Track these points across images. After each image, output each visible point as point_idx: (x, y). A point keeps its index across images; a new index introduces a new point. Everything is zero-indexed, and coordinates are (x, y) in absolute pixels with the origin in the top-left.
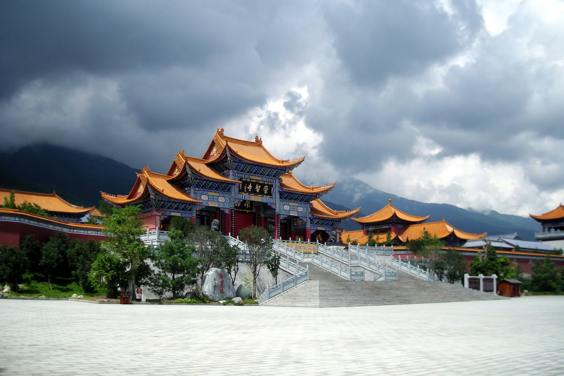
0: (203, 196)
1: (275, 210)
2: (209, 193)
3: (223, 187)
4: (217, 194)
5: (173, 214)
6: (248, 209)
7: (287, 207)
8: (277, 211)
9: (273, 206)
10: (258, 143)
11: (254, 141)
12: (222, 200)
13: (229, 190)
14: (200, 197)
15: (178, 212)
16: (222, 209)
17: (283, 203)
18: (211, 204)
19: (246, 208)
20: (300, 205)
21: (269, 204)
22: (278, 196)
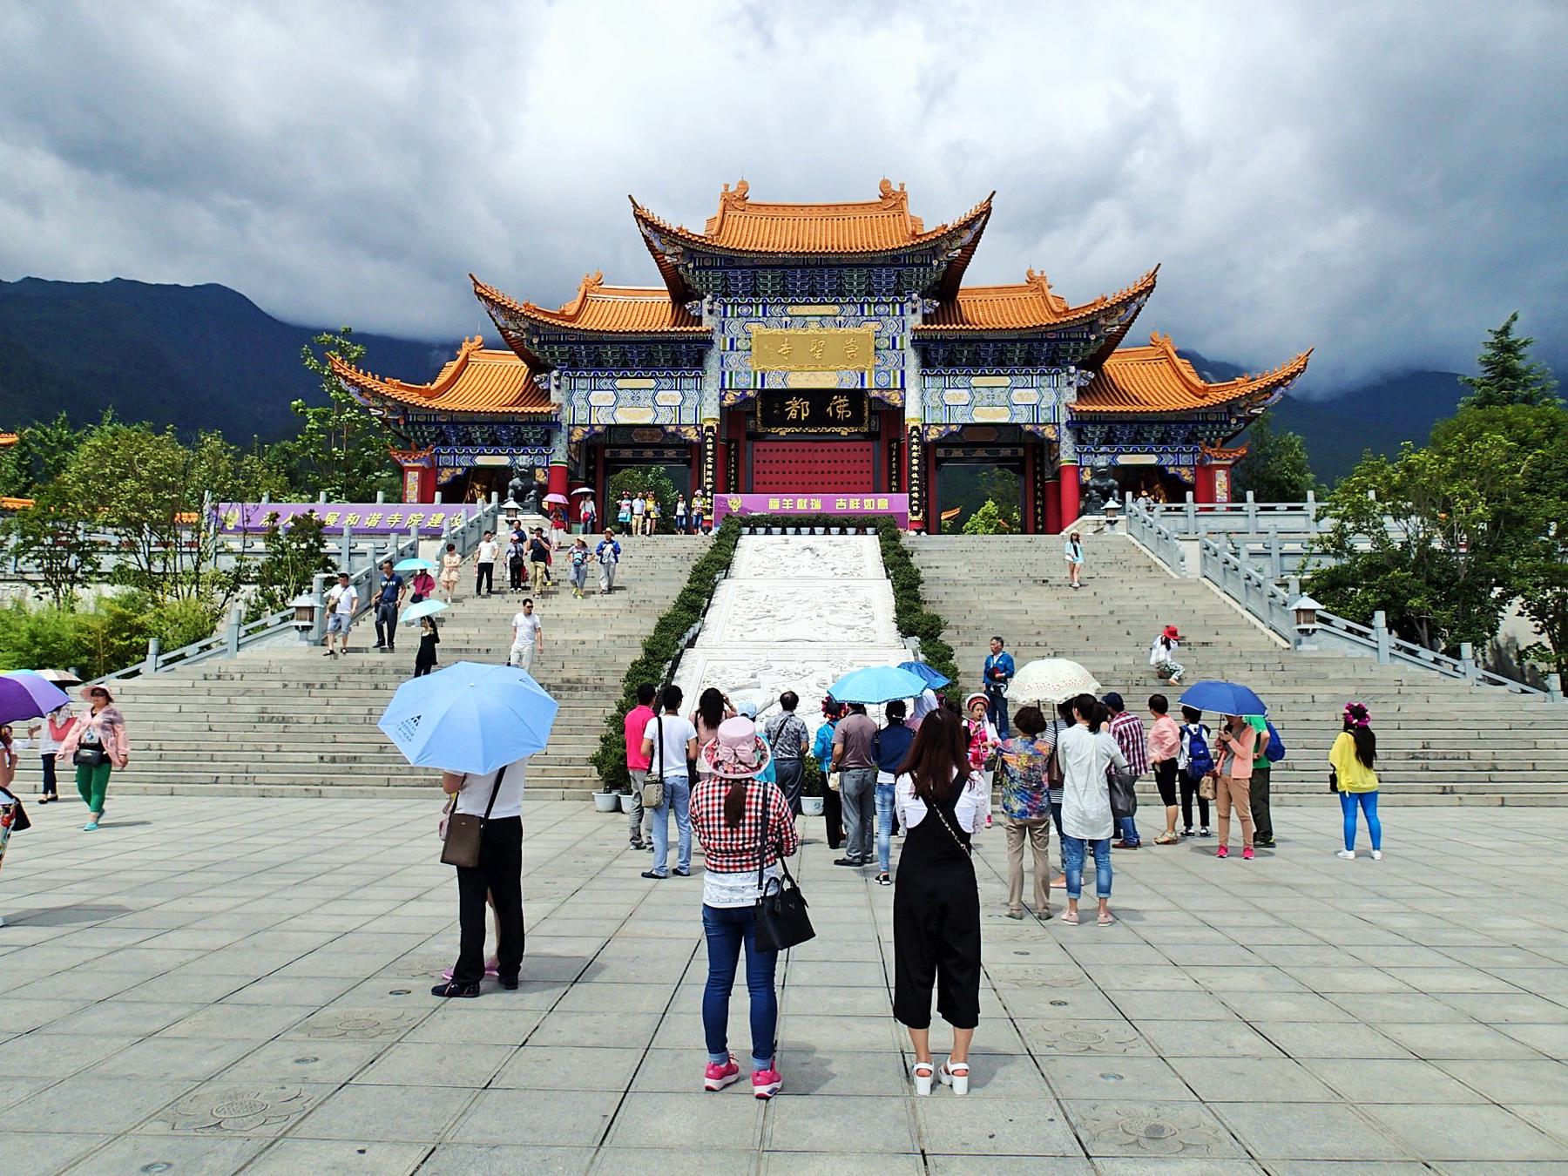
2: (619, 383)
3: (677, 355)
4: (652, 383)
5: (481, 461)
6: (847, 423)
8: (912, 415)
9: (895, 399)
10: (892, 199)
13: (699, 362)
14: (587, 400)
16: (671, 429)
17: (939, 381)
18: (627, 416)
19: (835, 422)
20: (1021, 381)
21: (875, 394)
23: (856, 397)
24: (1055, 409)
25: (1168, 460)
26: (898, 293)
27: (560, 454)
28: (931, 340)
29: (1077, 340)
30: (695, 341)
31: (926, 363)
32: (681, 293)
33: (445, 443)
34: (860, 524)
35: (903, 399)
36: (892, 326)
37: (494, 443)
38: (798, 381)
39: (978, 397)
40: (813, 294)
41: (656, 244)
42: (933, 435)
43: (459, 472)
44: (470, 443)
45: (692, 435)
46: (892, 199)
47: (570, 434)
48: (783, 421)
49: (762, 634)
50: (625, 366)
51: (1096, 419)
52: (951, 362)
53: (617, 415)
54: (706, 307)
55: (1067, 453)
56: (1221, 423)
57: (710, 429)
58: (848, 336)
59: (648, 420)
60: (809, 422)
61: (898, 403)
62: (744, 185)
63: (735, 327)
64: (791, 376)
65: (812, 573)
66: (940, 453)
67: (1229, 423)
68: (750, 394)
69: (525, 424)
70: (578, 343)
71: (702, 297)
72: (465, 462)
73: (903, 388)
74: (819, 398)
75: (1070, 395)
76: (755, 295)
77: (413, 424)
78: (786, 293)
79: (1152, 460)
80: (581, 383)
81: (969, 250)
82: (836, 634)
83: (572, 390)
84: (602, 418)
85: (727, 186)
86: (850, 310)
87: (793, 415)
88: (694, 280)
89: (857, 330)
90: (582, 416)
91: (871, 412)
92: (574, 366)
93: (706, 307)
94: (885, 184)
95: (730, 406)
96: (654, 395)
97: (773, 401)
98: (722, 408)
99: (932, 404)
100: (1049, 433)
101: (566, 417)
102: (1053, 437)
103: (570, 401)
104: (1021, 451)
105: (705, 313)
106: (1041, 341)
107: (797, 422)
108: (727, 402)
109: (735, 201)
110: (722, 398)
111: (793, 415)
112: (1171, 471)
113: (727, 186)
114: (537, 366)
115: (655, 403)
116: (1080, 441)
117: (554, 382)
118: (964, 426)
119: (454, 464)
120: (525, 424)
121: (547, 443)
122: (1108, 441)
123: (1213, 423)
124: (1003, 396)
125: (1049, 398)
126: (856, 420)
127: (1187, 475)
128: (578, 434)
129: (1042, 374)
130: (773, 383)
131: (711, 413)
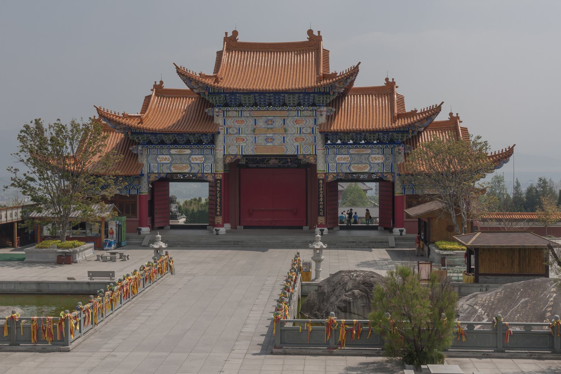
8: (321, 167)
10: (313, 43)
13: (213, 142)
16: (199, 175)
42: (330, 178)
46: (313, 43)
47: (149, 177)
53: (172, 169)
62: (235, 33)
85: (226, 33)
96: (190, 157)
98: (225, 165)
108: (227, 161)
109: (232, 43)
113: (226, 33)
115: (190, 161)
128: (153, 178)
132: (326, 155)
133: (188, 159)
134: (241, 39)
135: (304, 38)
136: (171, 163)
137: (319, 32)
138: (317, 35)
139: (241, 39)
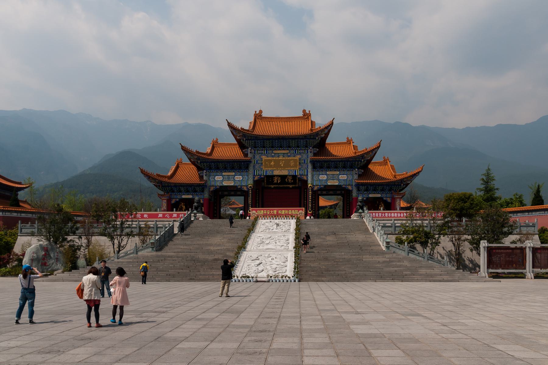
0: (216, 177)
1: (307, 181)
2: (223, 174)
4: (234, 174)
5: (184, 197)
6: (291, 184)
7: (323, 177)
8: (309, 181)
9: (305, 178)
11: (301, 114)
12: (239, 178)
14: (214, 178)
15: (188, 195)
16: (239, 187)
17: (318, 173)
18: (225, 184)
21: (299, 176)
22: (310, 167)
23: (294, 177)
24: (351, 181)
25: (384, 195)
26: (307, 147)
27: (206, 195)
28: (315, 161)
29: (358, 161)
30: (246, 161)
31: (314, 168)
32: (242, 146)
33: (173, 192)
34: (292, 216)
35: (307, 178)
36: (305, 156)
37: (187, 192)
38: (276, 173)
39: (329, 177)
40: (281, 147)
41: (234, 133)
42: (316, 188)
43: (177, 200)
44: (180, 191)
45: (245, 189)
48: (272, 183)
49: (261, 247)
50: (225, 169)
51: (363, 184)
52: (321, 167)
54: (249, 151)
55: (354, 194)
56: (399, 185)
57: (250, 187)
58: (291, 160)
59: (232, 184)
60: (280, 184)
61: (306, 179)
62: (261, 112)
63: (257, 157)
64: (275, 171)
65: (277, 231)
66: (319, 192)
67: (401, 185)
68: (262, 176)
69: (196, 186)
70: (212, 162)
71: (248, 148)
72: (179, 197)
73: (307, 175)
74: (283, 177)
75: (356, 177)
76: (264, 147)
77: (164, 186)
78: (273, 147)
79: (379, 196)
80: (212, 174)
81: (327, 135)
82: (278, 247)
83: (209, 176)
84: (219, 184)
85: (256, 112)
86: (292, 152)
87: (276, 181)
88: (246, 143)
89: (294, 158)
90: (213, 183)
91: (299, 181)
92: (210, 168)
93: (249, 151)
94: (304, 111)
95: (257, 180)
97: (270, 178)
98: (254, 181)
99: (317, 179)
100: (350, 188)
101: (209, 183)
102: (351, 189)
103: (209, 179)
104: (343, 192)
105: (249, 153)
106: (348, 161)
107: (277, 184)
108: (256, 179)
109: (258, 117)
110: (254, 178)
111: (276, 181)
112: (385, 199)
113: (256, 112)
114: (199, 169)
116: (359, 190)
117: (205, 174)
118: (325, 186)
119: (176, 197)
120: (196, 186)
121: (203, 191)
122: (367, 190)
123: (397, 185)
124: (337, 177)
125: (350, 177)
126: (294, 183)
127: (389, 200)
128: (212, 189)
129: (348, 170)
130: (269, 173)
131: (250, 183)
132: (313, 176)
133: (234, 178)
134: (264, 115)
135: (301, 114)
136: (223, 181)
137: (309, 111)
138: (308, 112)
139: (264, 115)
